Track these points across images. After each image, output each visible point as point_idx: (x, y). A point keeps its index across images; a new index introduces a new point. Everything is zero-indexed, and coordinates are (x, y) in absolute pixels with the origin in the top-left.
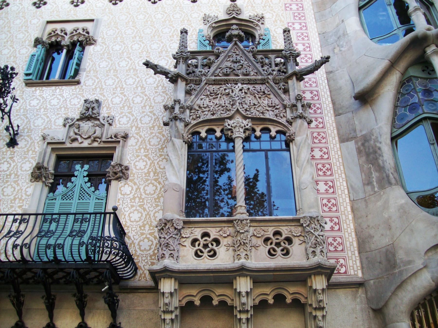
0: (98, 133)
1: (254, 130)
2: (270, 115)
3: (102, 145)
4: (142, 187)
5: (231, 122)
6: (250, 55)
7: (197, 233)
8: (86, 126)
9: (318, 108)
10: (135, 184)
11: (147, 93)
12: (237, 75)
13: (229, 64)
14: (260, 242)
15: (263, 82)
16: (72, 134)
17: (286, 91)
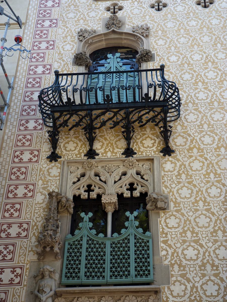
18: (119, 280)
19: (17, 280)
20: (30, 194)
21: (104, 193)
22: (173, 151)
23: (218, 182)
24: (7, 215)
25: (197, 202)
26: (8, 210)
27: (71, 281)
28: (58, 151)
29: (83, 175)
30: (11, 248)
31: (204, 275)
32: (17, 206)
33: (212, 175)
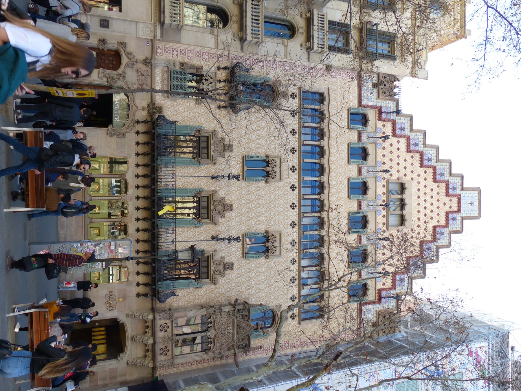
0: (216, 273)
1: (211, 338)
2: (217, 345)
3: (212, 275)
4: (193, 294)
5: (213, 331)
6: (247, 334)
7: (169, 324)
8: (221, 267)
9: (228, 358)
10: (194, 292)
11: (237, 288)
12: (237, 330)
13: (244, 325)
14: (165, 345)
15: (233, 340)
16: (216, 262)
17: (229, 349)
18: (172, 86)
19: (173, 56)
20: (204, 60)
21: (203, 84)
22: (219, 109)
23: (206, 122)
24: (197, 52)
25: (199, 114)
26: (198, 53)
27: (172, 72)
28: (221, 70)
29: (211, 78)
30: (185, 54)
31: (173, 111)
32: (200, 56)
33: (209, 120)
